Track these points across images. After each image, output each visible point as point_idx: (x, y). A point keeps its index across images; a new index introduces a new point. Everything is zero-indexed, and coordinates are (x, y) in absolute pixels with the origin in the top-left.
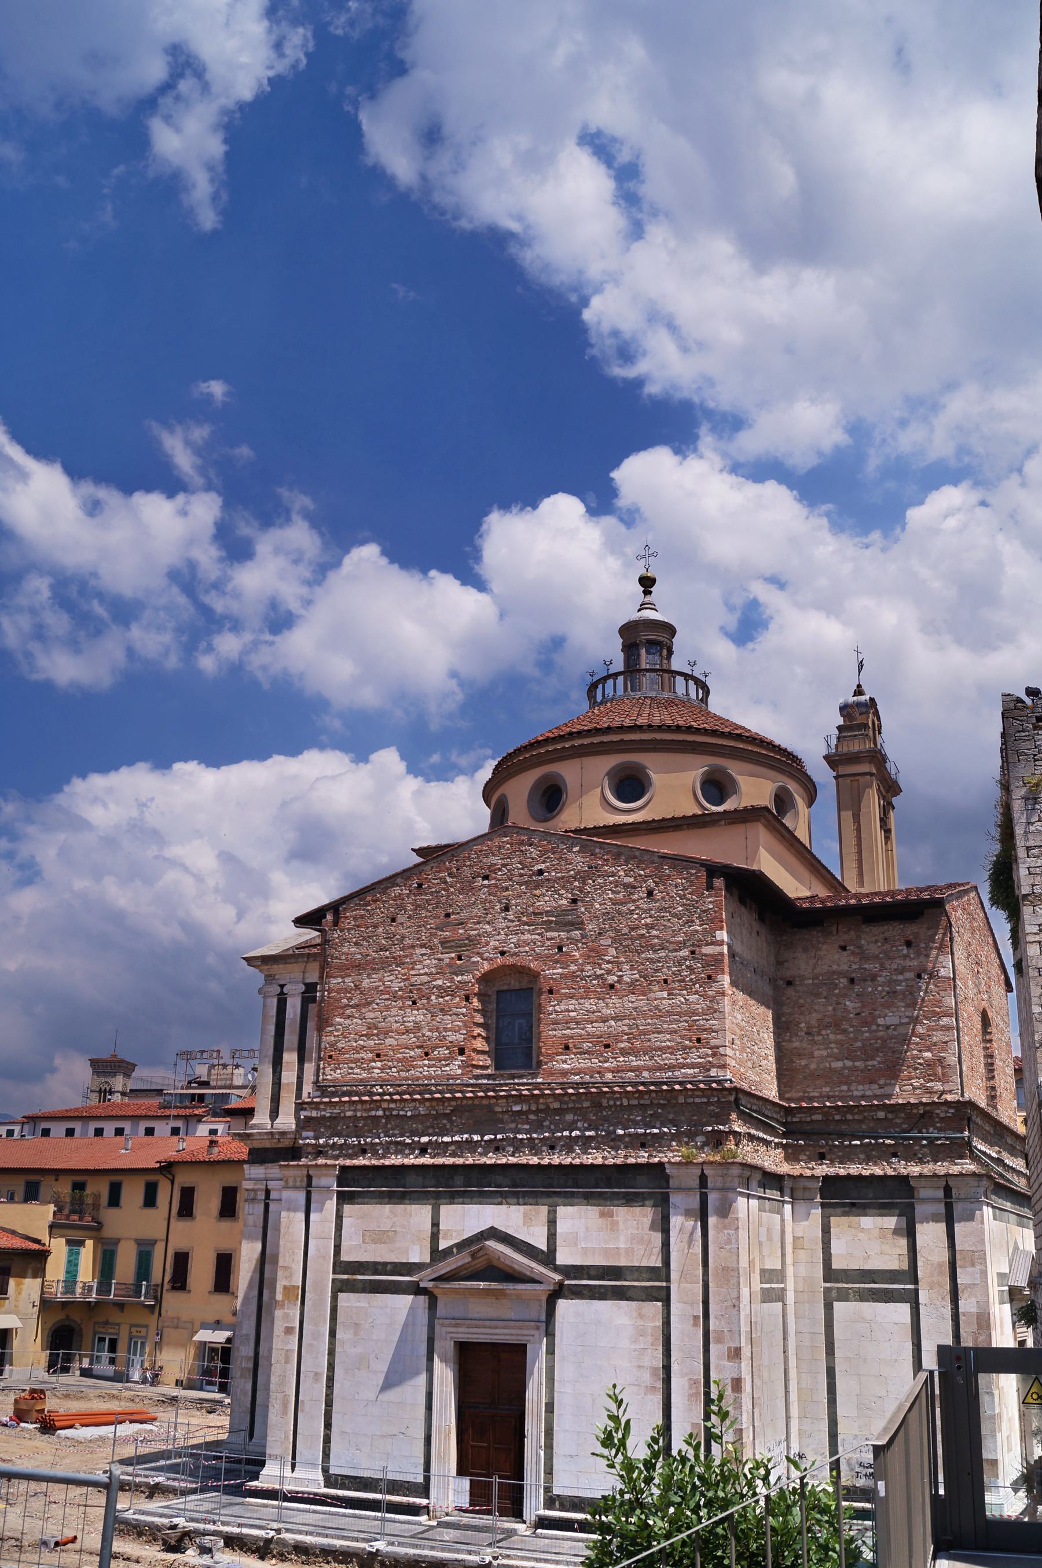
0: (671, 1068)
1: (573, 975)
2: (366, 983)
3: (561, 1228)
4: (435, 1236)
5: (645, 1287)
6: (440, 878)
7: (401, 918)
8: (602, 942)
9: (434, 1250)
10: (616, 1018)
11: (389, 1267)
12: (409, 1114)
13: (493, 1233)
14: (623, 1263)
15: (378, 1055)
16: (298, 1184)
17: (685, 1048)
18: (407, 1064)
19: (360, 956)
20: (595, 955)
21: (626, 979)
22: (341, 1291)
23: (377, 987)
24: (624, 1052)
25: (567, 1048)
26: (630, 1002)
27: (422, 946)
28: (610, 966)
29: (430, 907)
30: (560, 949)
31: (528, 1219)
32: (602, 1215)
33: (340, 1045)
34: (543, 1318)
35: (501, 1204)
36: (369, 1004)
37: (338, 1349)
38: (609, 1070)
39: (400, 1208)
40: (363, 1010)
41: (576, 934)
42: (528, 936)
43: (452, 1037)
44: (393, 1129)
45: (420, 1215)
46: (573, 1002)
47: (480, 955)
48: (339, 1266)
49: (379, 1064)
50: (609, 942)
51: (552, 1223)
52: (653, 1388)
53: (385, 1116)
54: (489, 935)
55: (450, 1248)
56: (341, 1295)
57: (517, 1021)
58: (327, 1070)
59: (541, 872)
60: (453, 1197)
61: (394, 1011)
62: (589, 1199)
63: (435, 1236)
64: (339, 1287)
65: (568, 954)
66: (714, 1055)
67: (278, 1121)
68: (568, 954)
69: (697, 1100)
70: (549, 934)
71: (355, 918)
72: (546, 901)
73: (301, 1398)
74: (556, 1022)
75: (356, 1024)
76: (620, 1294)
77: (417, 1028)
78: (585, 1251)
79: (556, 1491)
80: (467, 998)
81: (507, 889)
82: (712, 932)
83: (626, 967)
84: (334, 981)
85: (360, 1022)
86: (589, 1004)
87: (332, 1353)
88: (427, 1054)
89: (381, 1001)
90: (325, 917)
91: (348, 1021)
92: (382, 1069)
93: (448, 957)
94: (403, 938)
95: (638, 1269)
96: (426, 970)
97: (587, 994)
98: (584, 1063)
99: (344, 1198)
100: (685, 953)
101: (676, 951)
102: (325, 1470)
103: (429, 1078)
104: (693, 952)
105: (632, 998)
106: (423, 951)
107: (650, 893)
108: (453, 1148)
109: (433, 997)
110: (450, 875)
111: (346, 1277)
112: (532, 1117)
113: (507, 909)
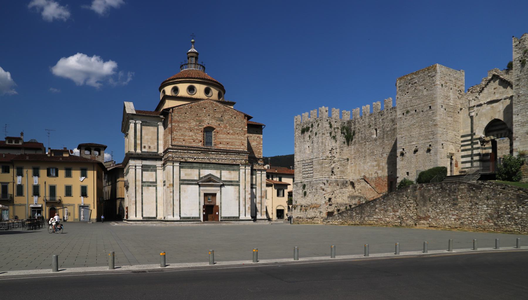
0: (239, 149)
1: (222, 130)
2: (180, 126)
3: (222, 174)
4: (199, 175)
5: (236, 184)
6: (196, 107)
7: (187, 113)
8: (227, 125)
9: (199, 177)
10: (229, 139)
11: (191, 180)
12: (192, 152)
13: (210, 174)
14: (232, 180)
15: (184, 140)
16: (171, 165)
17: (241, 145)
18: (190, 143)
19: (178, 120)
20: (225, 127)
21: (231, 132)
22: (181, 185)
23: (183, 127)
24: (231, 145)
25: (221, 143)
26: (231, 137)
27: (192, 120)
28: (228, 129)
29: (193, 112)
30: (219, 125)
31: (216, 173)
32: (229, 172)
33: (175, 137)
34: (220, 189)
35: (211, 170)
36: (181, 130)
37: (181, 195)
38: (228, 148)
39: (192, 170)
40: (180, 131)
41: (222, 123)
42: (213, 121)
43: (199, 138)
44: (188, 155)
45: (196, 171)
46: (222, 135)
47: (204, 123)
48: (180, 180)
49: (184, 142)
50: (228, 125)
51: (221, 173)
52: (237, 200)
53: (187, 152)
54: (206, 120)
55: (202, 177)
56: (181, 185)
57: (209, 137)
58: (173, 142)
59: (215, 110)
60: (203, 168)
61: (187, 132)
62: (227, 170)
63: (199, 175)
64: (180, 184)
65: (221, 126)
66: (245, 147)
67: (137, 151)
68: (221, 126)
69: (243, 154)
70: (217, 122)
71: (177, 111)
72: (217, 116)
73: (174, 204)
74: (219, 138)
75: (178, 134)
76: (232, 185)
77: (192, 136)
78: (226, 178)
79: (222, 216)
80: (202, 131)
81: (209, 111)
82: (245, 126)
83: (231, 130)
84: (173, 124)
85: (179, 133)
86: (225, 136)
87: (180, 196)
88: (194, 141)
89: (184, 130)
90: (170, 110)
91: (177, 133)
92: (185, 143)
93: (197, 123)
94: (188, 117)
95: (235, 181)
96: (193, 125)
97: (224, 134)
98: (223, 146)
99: (180, 167)
100: (241, 129)
101: (239, 128)
102: (180, 216)
103: (194, 146)
104: (242, 129)
105: (232, 136)
106: (193, 121)
107: (235, 118)
108: (201, 159)
109: (195, 130)
110: (198, 106)
111: (182, 182)
112: (215, 155)
113: (209, 115)
